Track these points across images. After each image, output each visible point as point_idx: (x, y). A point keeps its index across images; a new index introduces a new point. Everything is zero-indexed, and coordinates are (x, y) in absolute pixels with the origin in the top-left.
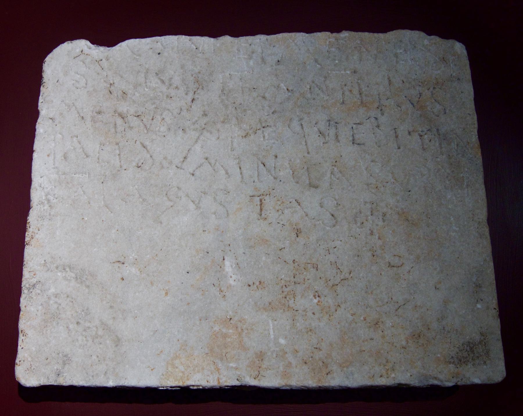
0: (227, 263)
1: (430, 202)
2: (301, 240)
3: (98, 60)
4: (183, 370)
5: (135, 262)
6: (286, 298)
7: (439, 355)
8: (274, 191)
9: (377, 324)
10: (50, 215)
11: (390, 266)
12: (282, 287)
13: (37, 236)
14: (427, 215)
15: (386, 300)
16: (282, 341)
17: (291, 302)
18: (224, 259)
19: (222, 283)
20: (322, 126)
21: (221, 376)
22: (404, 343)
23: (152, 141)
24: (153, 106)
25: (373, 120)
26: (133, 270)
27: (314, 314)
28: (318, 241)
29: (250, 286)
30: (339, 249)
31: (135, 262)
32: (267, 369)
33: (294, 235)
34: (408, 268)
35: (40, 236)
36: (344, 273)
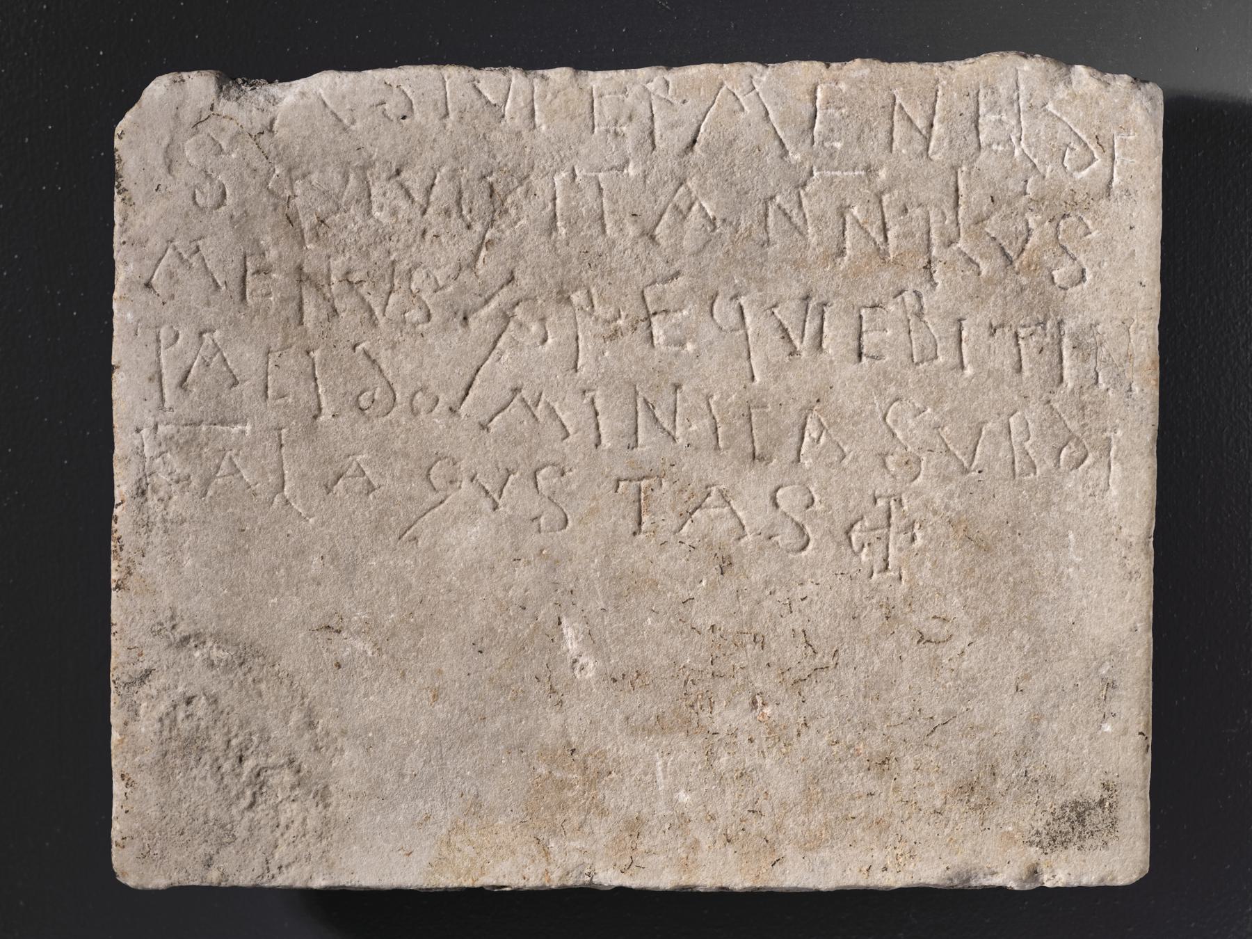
0: (569, 632)
1: (1024, 497)
2: (730, 583)
3: (253, 133)
4: (473, 855)
5: (367, 629)
6: (692, 706)
7: (1010, 829)
8: (674, 469)
9: (884, 763)
10: (164, 521)
11: (922, 639)
12: (686, 683)
13: (141, 570)
14: (1013, 527)
15: (906, 714)
16: (684, 797)
17: (704, 715)
18: (560, 623)
19: (554, 674)
20: (787, 314)
21: (552, 867)
22: (938, 803)
23: (393, 347)
24: (302, 383)
25: (909, 298)
26: (359, 645)
27: (751, 740)
28: (767, 583)
29: (615, 681)
30: (811, 602)
31: (367, 629)
32: (648, 852)
33: (715, 571)
34: (959, 645)
35: (152, 567)
36: (819, 655)
